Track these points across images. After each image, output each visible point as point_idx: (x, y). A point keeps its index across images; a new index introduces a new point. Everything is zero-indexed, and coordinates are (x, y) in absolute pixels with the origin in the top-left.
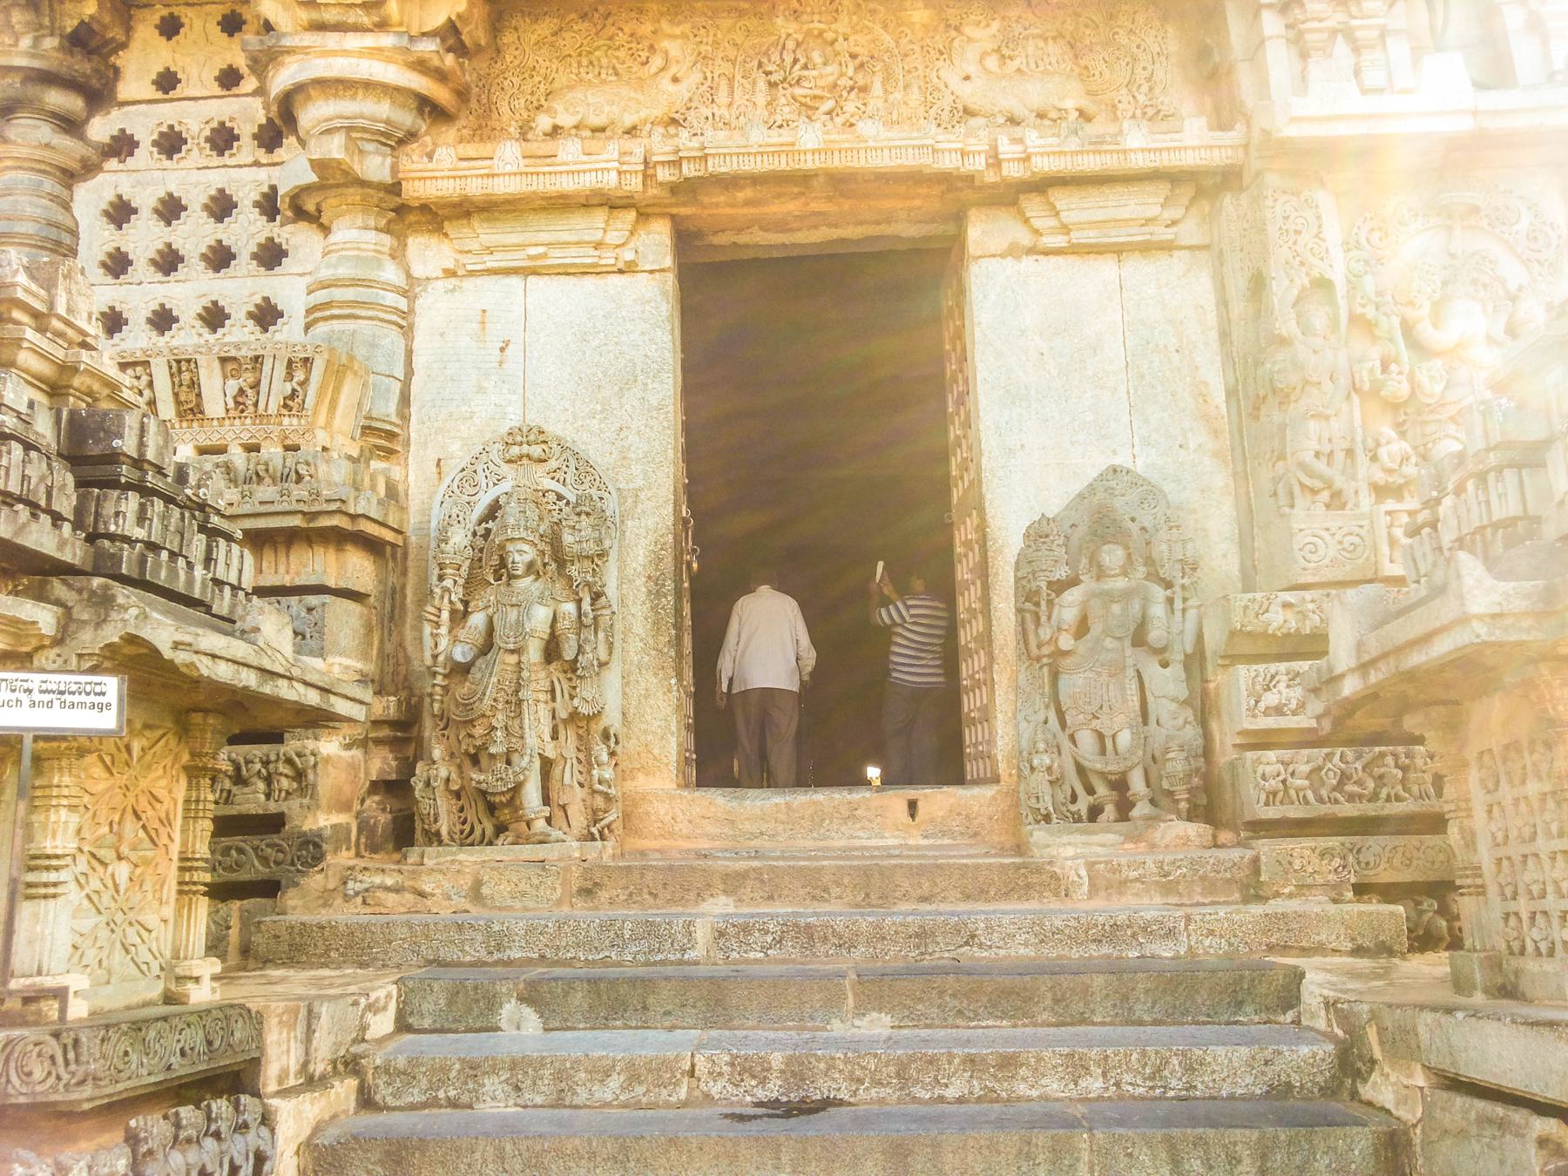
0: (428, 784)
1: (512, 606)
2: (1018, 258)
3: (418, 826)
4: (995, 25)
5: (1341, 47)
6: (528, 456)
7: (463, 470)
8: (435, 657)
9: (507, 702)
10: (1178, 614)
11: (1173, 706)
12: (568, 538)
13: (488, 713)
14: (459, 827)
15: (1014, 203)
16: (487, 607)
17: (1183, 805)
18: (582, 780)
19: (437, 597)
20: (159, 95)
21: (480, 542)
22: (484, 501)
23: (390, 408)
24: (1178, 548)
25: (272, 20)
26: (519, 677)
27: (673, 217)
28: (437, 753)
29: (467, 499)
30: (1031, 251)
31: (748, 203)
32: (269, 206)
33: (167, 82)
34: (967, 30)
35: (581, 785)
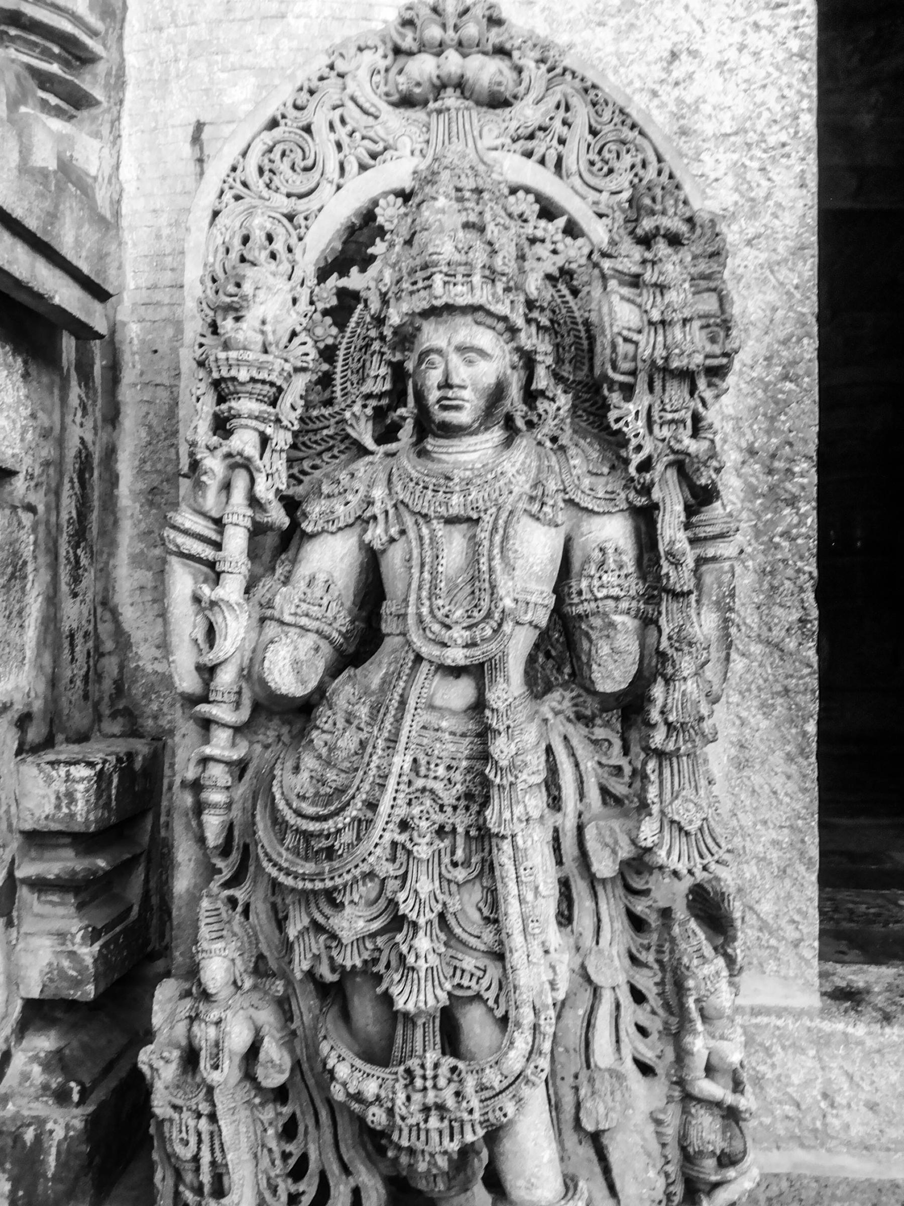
1: (451, 521)
6: (461, 85)
7: (273, 124)
8: (208, 672)
9: (441, 832)
13: (386, 869)
14: (285, 1187)
16: (364, 521)
18: (648, 1055)
19: (212, 484)
21: (327, 331)
26: (484, 756)
29: (287, 205)
35: (646, 1069)
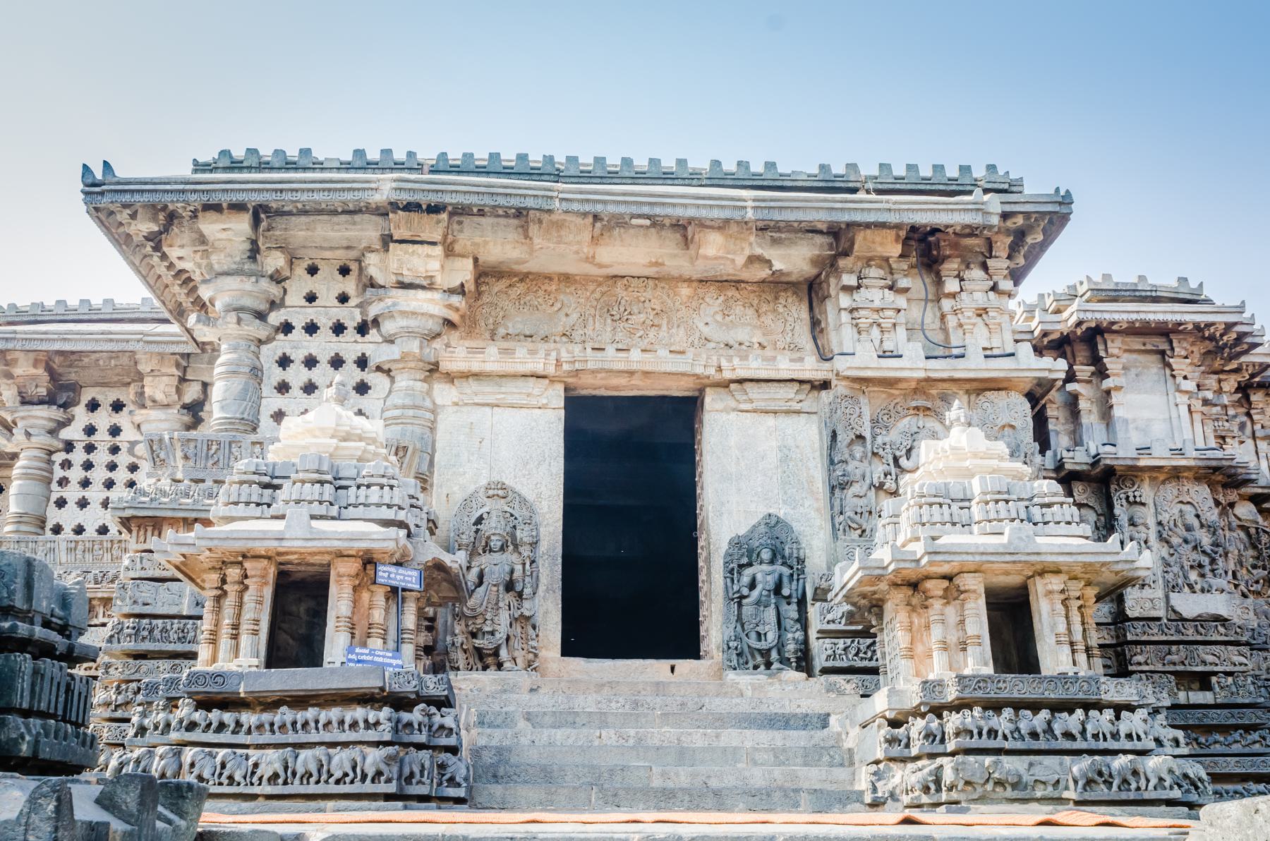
0: (453, 644)
2: (728, 413)
3: (447, 664)
4: (722, 299)
5: (875, 332)
10: (795, 582)
11: (792, 622)
12: (518, 533)
15: (727, 386)
17: (794, 664)
20: (307, 304)
22: (478, 515)
23: (425, 468)
24: (795, 551)
25: (374, 276)
27: (565, 382)
28: (457, 631)
30: (734, 410)
31: (601, 379)
32: (362, 362)
33: (311, 298)
34: (707, 300)
